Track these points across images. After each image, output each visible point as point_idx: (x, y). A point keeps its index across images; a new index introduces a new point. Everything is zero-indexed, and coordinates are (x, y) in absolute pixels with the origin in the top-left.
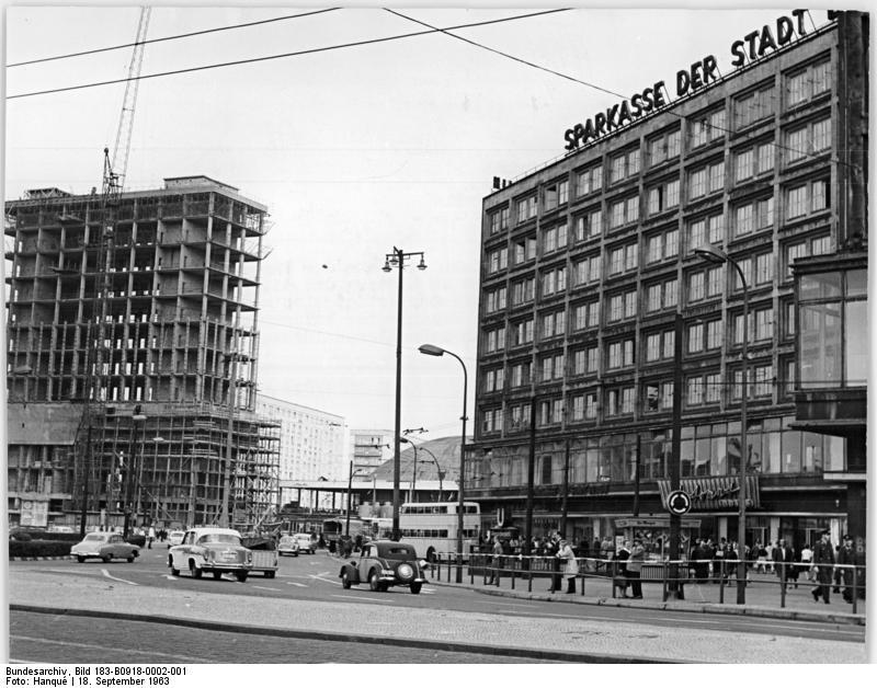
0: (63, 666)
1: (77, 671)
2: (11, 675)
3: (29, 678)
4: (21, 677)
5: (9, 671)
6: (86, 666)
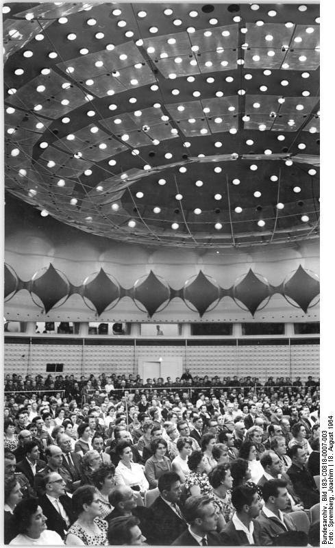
1: (325, 500)
2: (327, 541)
3: (329, 529)
4: (328, 535)
5: (324, 543)
6: (321, 494)
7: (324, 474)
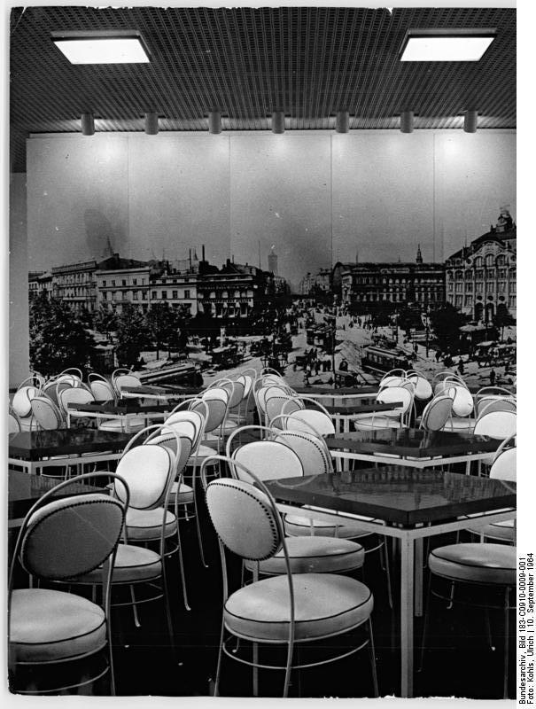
0: (519, 658)
1: (522, 646)
2: (526, 700)
4: (527, 692)
5: (522, 702)
6: (518, 639)
7: (522, 614)
